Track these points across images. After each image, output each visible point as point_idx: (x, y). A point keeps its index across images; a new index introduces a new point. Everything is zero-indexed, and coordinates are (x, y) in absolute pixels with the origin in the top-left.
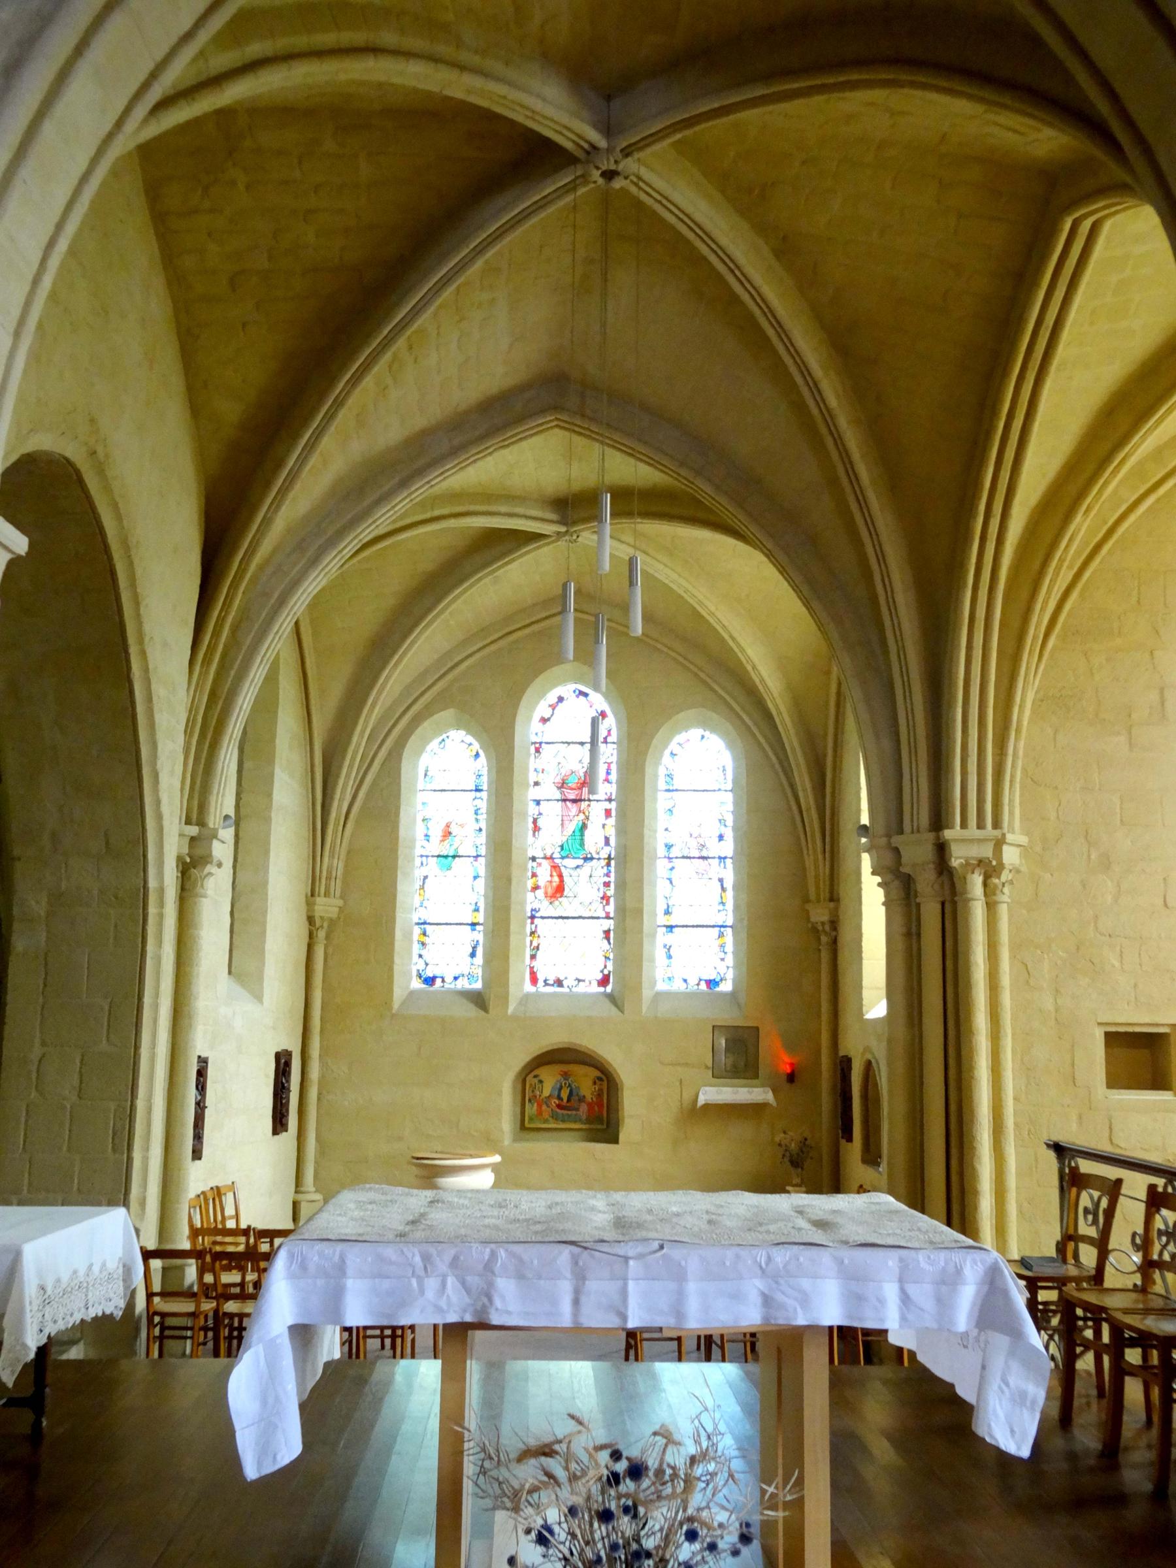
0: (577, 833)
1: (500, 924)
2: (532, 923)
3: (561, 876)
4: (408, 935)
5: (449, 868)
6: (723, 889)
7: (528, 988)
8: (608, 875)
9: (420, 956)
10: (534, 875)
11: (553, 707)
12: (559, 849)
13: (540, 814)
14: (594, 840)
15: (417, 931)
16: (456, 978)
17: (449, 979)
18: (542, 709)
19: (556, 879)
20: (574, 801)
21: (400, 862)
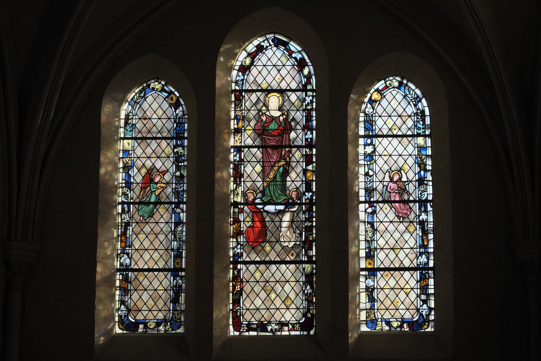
0: (278, 179)
1: (202, 267)
2: (235, 268)
3: (263, 221)
4: (109, 281)
5: (151, 215)
6: (425, 233)
7: (232, 332)
8: (309, 219)
9: (122, 302)
10: (237, 221)
11: (253, 56)
12: (259, 195)
13: (241, 160)
14: (295, 180)
15: (119, 276)
16: (158, 324)
17: (152, 325)
18: (242, 57)
19: (258, 224)
20: (274, 148)
21: (100, 207)
